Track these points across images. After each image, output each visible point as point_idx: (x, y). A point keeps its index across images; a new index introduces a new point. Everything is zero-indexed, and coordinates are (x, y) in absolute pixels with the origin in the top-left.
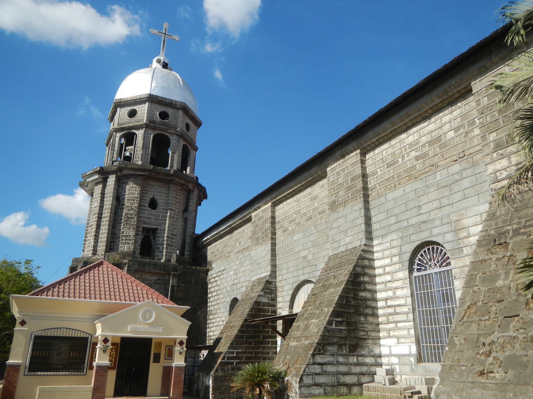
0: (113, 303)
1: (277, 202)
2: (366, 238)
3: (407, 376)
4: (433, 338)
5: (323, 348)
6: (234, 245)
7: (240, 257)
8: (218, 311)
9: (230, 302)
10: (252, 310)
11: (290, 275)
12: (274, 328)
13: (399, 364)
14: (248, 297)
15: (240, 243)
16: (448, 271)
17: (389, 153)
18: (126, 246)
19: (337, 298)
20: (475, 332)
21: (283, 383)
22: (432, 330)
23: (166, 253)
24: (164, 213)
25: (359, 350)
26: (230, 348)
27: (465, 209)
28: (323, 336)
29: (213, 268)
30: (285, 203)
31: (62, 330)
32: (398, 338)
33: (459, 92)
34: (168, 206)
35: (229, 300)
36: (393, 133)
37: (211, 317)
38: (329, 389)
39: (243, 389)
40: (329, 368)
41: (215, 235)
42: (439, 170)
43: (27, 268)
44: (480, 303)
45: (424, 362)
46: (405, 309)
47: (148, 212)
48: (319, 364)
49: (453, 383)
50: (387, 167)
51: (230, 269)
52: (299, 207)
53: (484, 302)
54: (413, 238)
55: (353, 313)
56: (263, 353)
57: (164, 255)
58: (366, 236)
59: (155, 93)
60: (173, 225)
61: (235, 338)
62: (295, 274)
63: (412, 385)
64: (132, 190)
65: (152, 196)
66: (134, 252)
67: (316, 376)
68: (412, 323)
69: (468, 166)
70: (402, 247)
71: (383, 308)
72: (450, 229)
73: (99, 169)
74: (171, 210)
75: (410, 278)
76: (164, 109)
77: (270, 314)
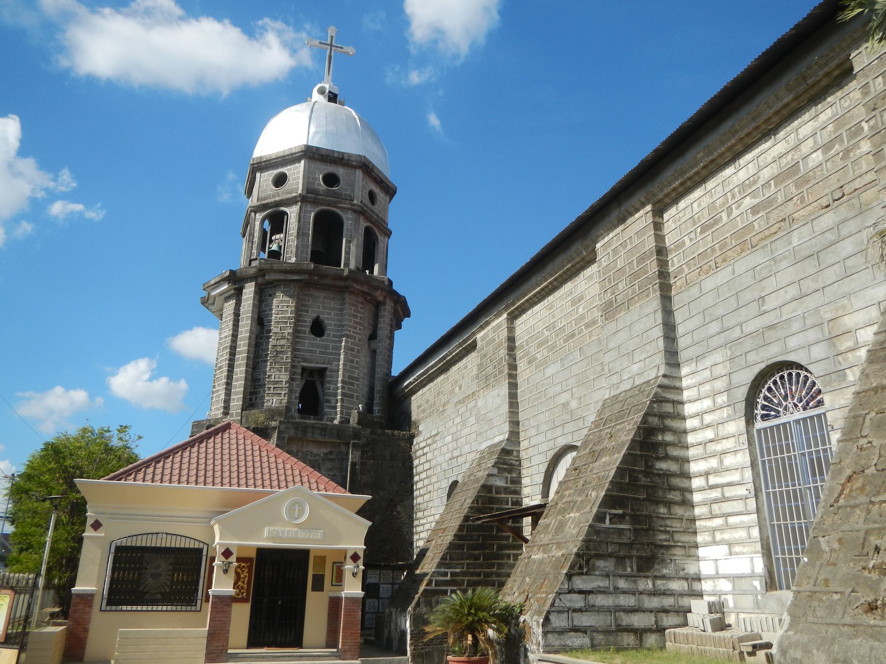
0: (243, 491)
1: (516, 312)
2: (667, 364)
3: (748, 615)
4: (796, 543)
5: (587, 563)
6: (452, 392)
7: (461, 411)
8: (430, 505)
9: (447, 489)
10: (477, 501)
11: (541, 438)
12: (518, 532)
13: (733, 593)
14: (472, 478)
15: (460, 388)
16: (819, 416)
17: (704, 205)
18: (276, 398)
19: (613, 472)
20: (861, 525)
21: (518, 624)
22: (793, 528)
23: (342, 408)
24: (336, 342)
25: (656, 566)
26: (439, 565)
27: (848, 295)
28: (587, 542)
29: (421, 432)
30: (530, 312)
31: (160, 536)
32: (730, 544)
33: (827, 74)
34: (342, 331)
35: (446, 484)
36: (710, 167)
37: (419, 515)
38: (600, 637)
39: (445, 635)
40: (599, 599)
41: (422, 375)
42: (796, 227)
43: (121, 439)
44: (872, 470)
45: (781, 589)
46: (741, 491)
47: (310, 342)
48: (581, 592)
49: (815, 627)
50: (702, 232)
51: (446, 433)
53: (880, 467)
54: (752, 357)
55: (644, 500)
56: (498, 575)
57: (339, 412)
58: (666, 359)
59: (314, 143)
60: (352, 361)
61: (449, 548)
62: (549, 435)
63: (756, 631)
64: (282, 307)
65: (315, 315)
66: (288, 408)
67: (575, 614)
68: (754, 517)
69: (852, 214)
70: (733, 376)
71: (701, 490)
72: (820, 336)
73: (228, 274)
74: (348, 336)
75: (748, 432)
77: (510, 506)
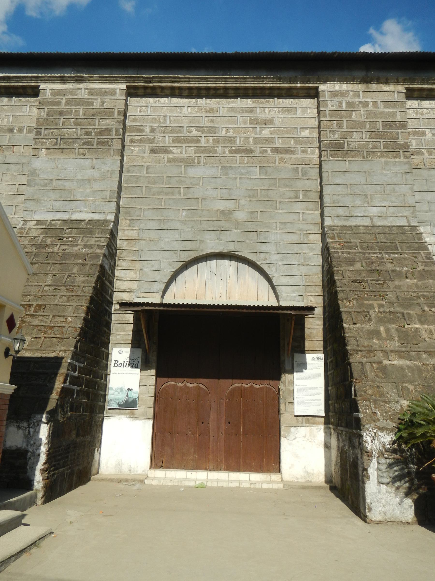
52: (212, 121)
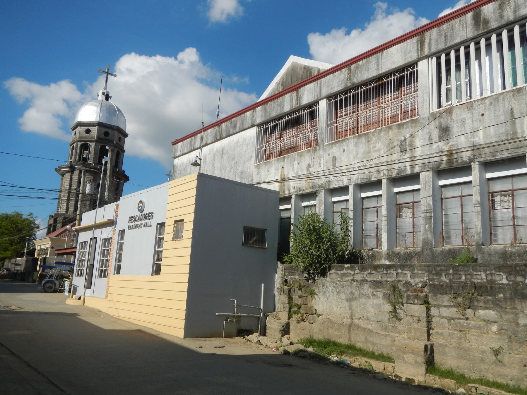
76: (107, 130)
